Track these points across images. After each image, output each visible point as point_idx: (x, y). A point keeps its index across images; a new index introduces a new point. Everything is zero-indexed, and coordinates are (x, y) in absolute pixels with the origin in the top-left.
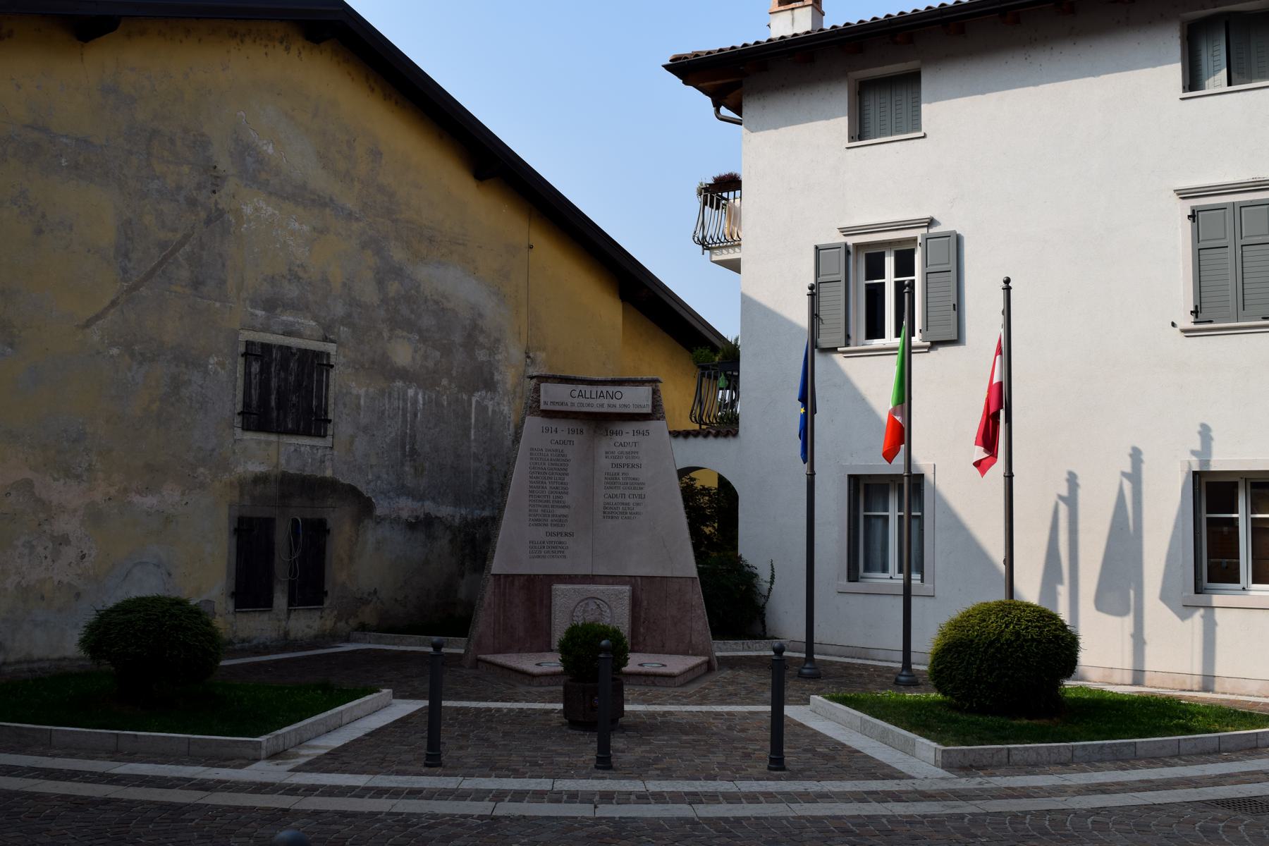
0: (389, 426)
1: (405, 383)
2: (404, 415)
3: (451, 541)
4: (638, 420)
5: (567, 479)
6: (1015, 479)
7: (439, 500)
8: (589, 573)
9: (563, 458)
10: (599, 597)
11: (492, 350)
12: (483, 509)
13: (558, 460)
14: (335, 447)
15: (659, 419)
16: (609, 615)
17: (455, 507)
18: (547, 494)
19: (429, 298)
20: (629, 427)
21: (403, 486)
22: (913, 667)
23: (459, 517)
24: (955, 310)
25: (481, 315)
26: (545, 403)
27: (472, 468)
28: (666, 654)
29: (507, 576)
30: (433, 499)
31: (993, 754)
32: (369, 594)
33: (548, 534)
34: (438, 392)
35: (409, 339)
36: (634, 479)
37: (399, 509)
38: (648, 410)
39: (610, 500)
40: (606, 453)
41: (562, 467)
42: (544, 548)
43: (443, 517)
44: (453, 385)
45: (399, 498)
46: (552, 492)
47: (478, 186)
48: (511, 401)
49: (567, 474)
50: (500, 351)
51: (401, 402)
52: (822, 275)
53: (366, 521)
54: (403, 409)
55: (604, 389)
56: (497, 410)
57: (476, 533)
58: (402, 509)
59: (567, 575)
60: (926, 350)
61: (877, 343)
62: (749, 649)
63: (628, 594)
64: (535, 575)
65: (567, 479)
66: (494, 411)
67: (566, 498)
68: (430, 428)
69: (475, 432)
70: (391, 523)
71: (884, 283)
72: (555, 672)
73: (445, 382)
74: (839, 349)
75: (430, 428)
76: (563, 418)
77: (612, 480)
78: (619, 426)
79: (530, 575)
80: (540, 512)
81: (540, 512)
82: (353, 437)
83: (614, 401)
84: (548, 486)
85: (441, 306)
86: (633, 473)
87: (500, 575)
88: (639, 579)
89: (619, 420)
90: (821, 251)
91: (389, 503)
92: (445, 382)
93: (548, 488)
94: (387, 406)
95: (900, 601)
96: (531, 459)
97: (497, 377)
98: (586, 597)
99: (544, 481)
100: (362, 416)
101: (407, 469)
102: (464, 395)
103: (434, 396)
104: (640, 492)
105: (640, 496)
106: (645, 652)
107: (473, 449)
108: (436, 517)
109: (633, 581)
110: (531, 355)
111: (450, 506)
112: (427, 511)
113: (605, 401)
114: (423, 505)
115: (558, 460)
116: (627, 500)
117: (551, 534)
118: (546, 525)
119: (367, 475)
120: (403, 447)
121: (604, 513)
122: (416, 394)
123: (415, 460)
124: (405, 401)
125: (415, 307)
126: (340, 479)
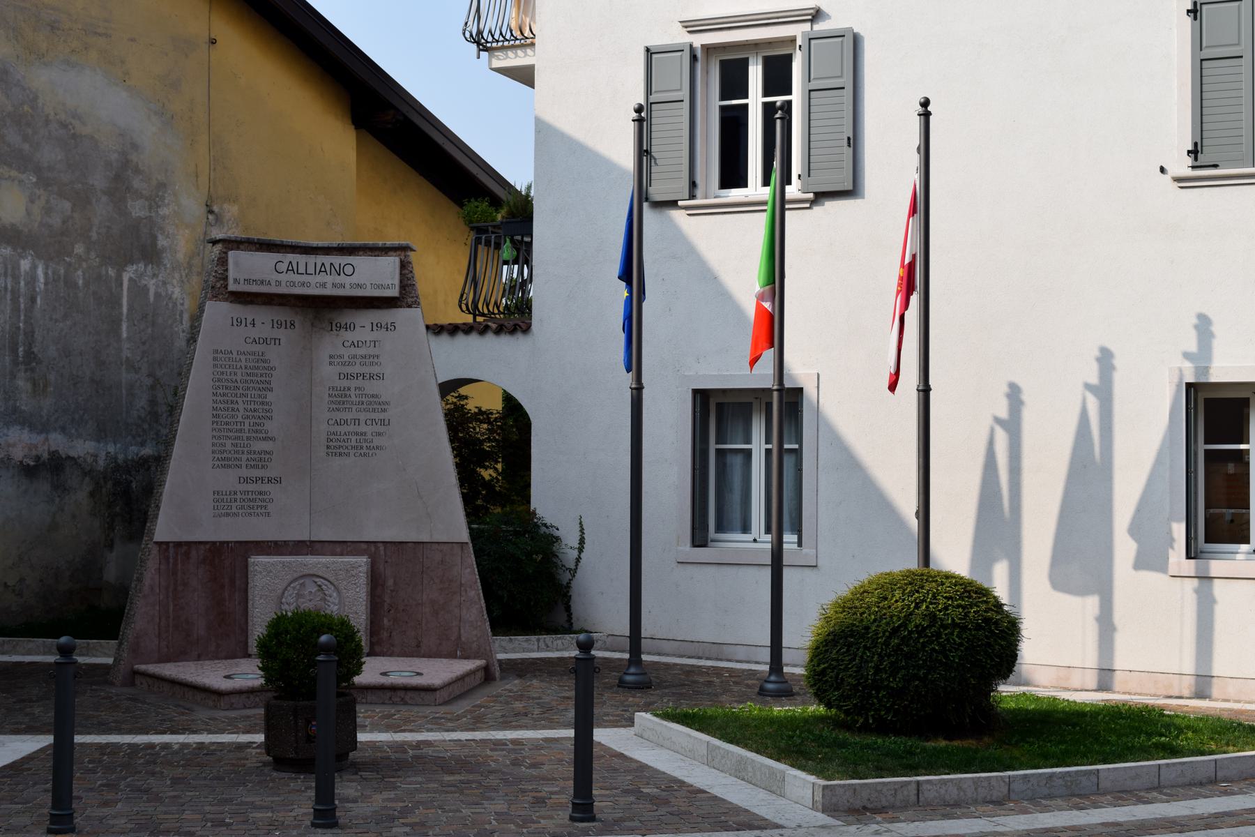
1: (14, 249)
2: (15, 300)
3: (92, 495)
4: (378, 307)
5: (270, 397)
6: (933, 395)
7: (73, 431)
8: (306, 538)
9: (266, 365)
10: (320, 574)
11: (154, 201)
12: (143, 444)
13: (258, 368)
15: (410, 306)
16: (337, 601)
17: (99, 442)
19: (51, 117)
20: (366, 318)
21: (15, 410)
22: (786, 670)
23: (104, 458)
24: (849, 146)
25: (135, 146)
26: (235, 280)
27: (124, 381)
28: (424, 657)
29: (179, 544)
30: (63, 429)
31: (896, 790)
33: (242, 480)
34: (70, 264)
35: (21, 181)
36: (373, 396)
37: (9, 445)
38: (394, 292)
40: (331, 357)
41: (263, 379)
42: (235, 501)
43: (79, 457)
44: (93, 255)
45: (8, 429)
46: (248, 417)
48: (185, 280)
49: (271, 390)
50: (166, 201)
51: (9, 280)
52: (655, 92)
54: (13, 291)
55: (327, 260)
56: (163, 294)
57: (131, 482)
58: (14, 445)
59: (271, 542)
60: (808, 205)
61: (735, 194)
62: (548, 648)
63: (364, 569)
64: (222, 543)
65: (270, 397)
66: (157, 295)
67: (268, 425)
68: (56, 321)
69: (128, 327)
71: (746, 106)
72: (253, 688)
73: (79, 249)
74: (680, 203)
75: (56, 321)
76: (264, 304)
77: (340, 398)
78: (348, 317)
79: (214, 543)
80: (229, 447)
81: (229, 447)
83: (341, 279)
84: (241, 407)
85: (72, 131)
86: (371, 387)
87: (167, 543)
88: (382, 548)
89: (351, 308)
90: (654, 56)
92: (79, 249)
95: (767, 574)
96: (215, 366)
97: (162, 242)
98: (301, 574)
99: (235, 399)
101: (20, 383)
102: (110, 269)
103: (62, 271)
104: (382, 416)
105: (383, 422)
106: (391, 655)
107: (126, 353)
108: (69, 457)
109: (373, 549)
110: (215, 208)
111: (91, 441)
112: (53, 449)
113: (328, 279)
114: (47, 439)
115: (258, 368)
116: (363, 428)
117: (246, 480)
118: (239, 467)
120: (14, 351)
121: (328, 447)
122: (34, 267)
123: (33, 370)
124: (16, 278)
125: (30, 131)
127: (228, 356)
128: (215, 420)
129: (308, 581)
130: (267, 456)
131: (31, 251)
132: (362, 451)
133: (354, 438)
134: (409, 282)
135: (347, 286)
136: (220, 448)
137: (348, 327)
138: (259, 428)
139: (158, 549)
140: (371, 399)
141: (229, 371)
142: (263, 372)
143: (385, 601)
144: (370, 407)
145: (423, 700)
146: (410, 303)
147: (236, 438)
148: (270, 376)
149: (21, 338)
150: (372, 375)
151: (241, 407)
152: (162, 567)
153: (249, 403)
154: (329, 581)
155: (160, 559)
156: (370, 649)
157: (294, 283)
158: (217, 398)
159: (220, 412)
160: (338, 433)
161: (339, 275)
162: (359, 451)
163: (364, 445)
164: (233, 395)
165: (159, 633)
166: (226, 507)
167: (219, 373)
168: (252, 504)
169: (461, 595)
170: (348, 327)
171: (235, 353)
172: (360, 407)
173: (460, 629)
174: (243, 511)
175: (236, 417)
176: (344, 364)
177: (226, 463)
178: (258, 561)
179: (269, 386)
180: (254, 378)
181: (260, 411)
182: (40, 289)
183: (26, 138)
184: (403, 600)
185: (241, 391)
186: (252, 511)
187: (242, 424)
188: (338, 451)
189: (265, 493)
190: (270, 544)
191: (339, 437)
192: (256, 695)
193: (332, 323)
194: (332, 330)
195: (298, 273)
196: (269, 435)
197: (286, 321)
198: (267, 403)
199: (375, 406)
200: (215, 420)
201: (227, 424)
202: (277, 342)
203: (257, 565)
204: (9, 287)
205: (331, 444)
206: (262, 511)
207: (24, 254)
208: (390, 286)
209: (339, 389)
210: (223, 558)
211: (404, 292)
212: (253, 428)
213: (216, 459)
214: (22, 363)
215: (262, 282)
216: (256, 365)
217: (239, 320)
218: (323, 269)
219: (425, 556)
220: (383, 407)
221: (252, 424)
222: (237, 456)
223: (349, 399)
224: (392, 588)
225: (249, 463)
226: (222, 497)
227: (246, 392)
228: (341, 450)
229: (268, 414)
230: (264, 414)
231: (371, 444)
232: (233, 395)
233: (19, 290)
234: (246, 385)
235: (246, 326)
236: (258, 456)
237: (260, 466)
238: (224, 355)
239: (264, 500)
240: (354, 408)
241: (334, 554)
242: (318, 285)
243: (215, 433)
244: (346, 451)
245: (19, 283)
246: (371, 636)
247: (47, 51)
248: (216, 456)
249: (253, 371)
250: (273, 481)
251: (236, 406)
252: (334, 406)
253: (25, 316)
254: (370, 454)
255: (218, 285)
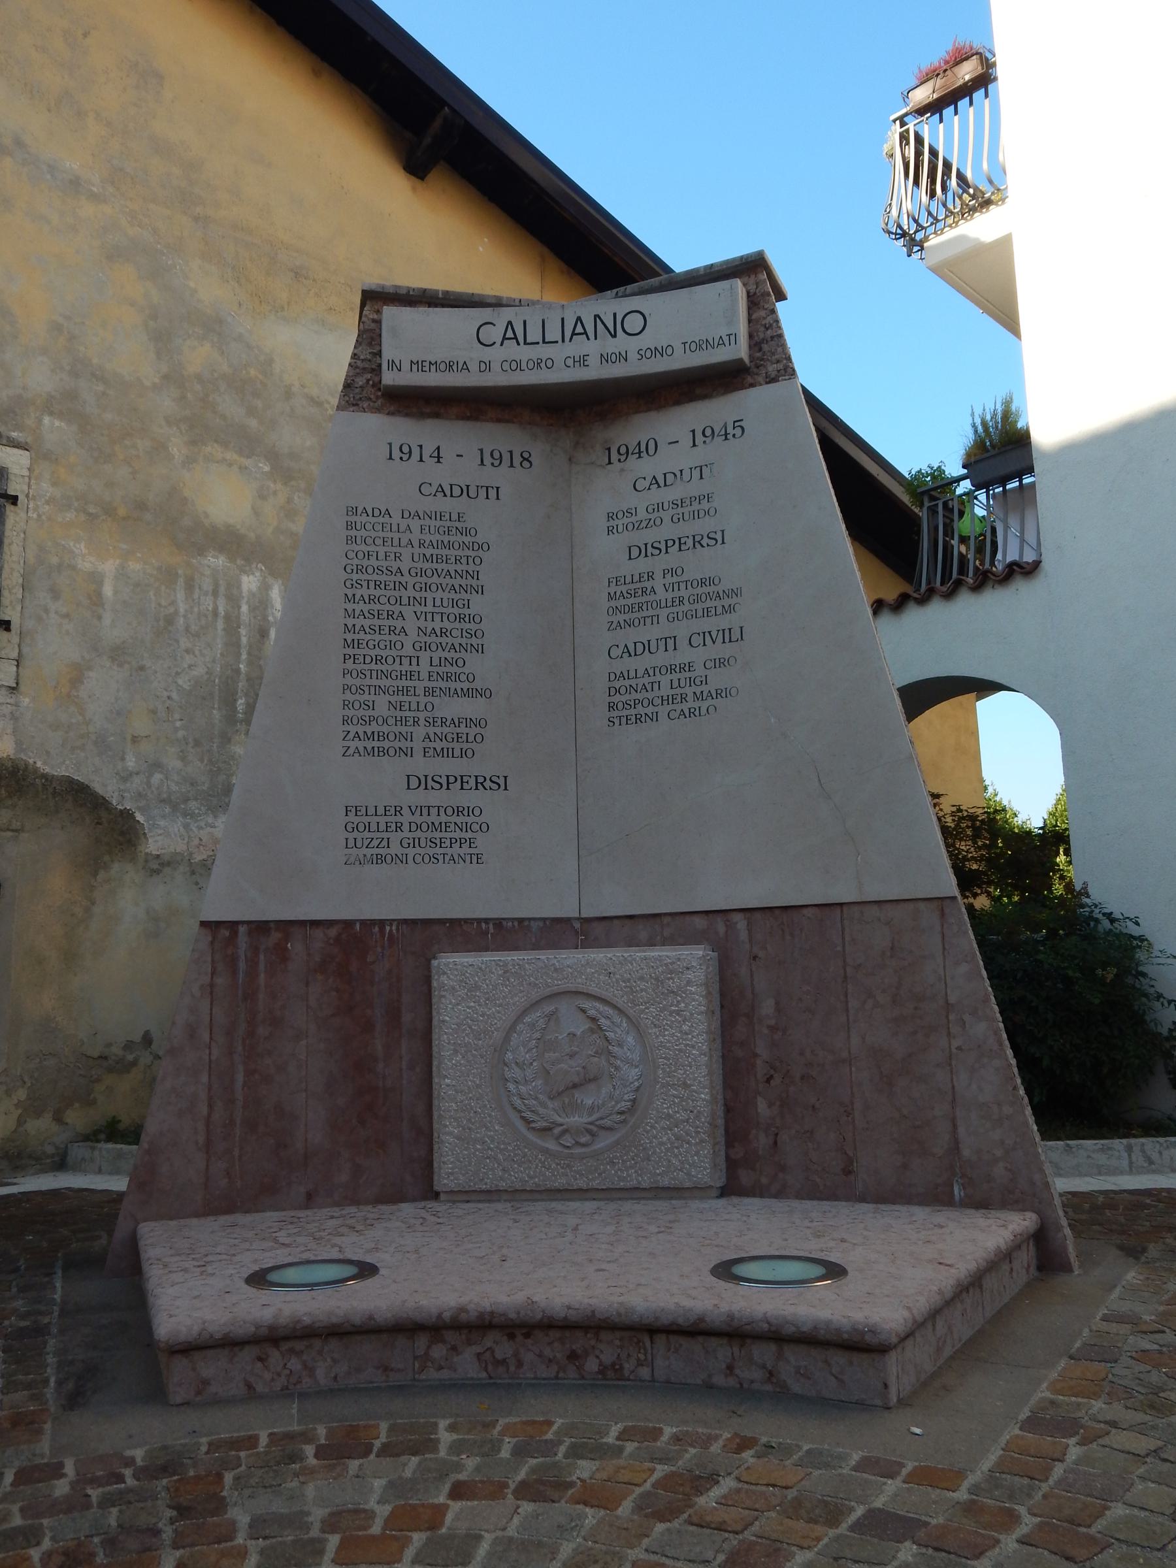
0: (187, 651)
5: (478, 604)
9: (467, 539)
10: (593, 989)
13: (450, 545)
14: (22, 688)
15: (772, 380)
16: (636, 1056)
18: (411, 652)
28: (863, 1199)
29: (260, 928)
32: (129, 1046)
33: (414, 783)
36: (702, 583)
39: (630, 664)
40: (610, 517)
41: (459, 568)
42: (399, 827)
45: (215, 817)
46: (427, 647)
47: (414, 189)
49: (480, 590)
53: (116, 867)
54: (227, 618)
59: (487, 921)
62: (1151, 1166)
63: (698, 975)
64: (367, 924)
65: (478, 604)
67: (474, 664)
70: (193, 873)
72: (272, 1328)
79: (348, 924)
82: (77, 675)
83: (621, 343)
84: (411, 625)
86: (697, 564)
87: (233, 925)
88: (741, 922)
91: (186, 826)
93: (413, 633)
94: (182, 607)
98: (548, 991)
99: (397, 609)
100: (107, 619)
104: (724, 622)
105: (727, 636)
106: (779, 1195)
109: (721, 928)
113: (591, 348)
115: (450, 545)
116: (685, 655)
117: (424, 782)
119: (123, 759)
121: (611, 707)
122: (265, 588)
124: (234, 600)
125: (259, 403)
126: (39, 764)
127: (381, 519)
128: (350, 651)
129: (565, 1007)
130: (473, 731)
131: (260, 565)
132: (685, 707)
133: (665, 680)
134: (769, 332)
135: (633, 356)
136: (361, 713)
137: (643, 448)
138: (454, 669)
139: (210, 939)
140: (699, 590)
141: (382, 551)
142: (460, 553)
143: (756, 1055)
144: (699, 606)
145: (841, 1382)
146: (773, 375)
147: (405, 691)
148: (477, 561)
149: (242, 684)
150: (698, 538)
151: (411, 625)
152: (219, 981)
153: (429, 616)
154: (615, 1007)
155: (213, 961)
156: (728, 1179)
157: (519, 364)
158: (355, 606)
159: (362, 635)
160: (632, 674)
161: (614, 336)
162: (678, 707)
163: (689, 691)
164: (393, 601)
165: (209, 1143)
166: (375, 843)
167: (360, 555)
168: (438, 835)
169: (949, 1034)
170: (643, 448)
171: (396, 516)
172: (675, 609)
173: (955, 1126)
174: (418, 850)
175: (399, 646)
176: (637, 527)
177: (376, 744)
178: (447, 965)
179: (474, 583)
180: (439, 567)
181: (455, 633)
182: (274, 617)
183: (251, 412)
184: (802, 1054)
185: (411, 592)
186: (438, 850)
187: (414, 661)
188: (633, 712)
189: (470, 811)
190: (484, 925)
191: (633, 682)
192: (292, 1351)
193: (609, 449)
194: (610, 463)
195: (525, 343)
196: (478, 684)
197: (511, 452)
198: (472, 619)
199: (709, 604)
200: (350, 651)
201: (377, 660)
202: (492, 493)
203: (444, 973)
204: (221, 610)
205: (617, 698)
206: (462, 852)
207: (247, 568)
208: (726, 339)
209: (628, 579)
210: (370, 959)
211: (758, 355)
212: (441, 670)
213: (351, 736)
214: (241, 722)
215: (450, 366)
216: (446, 539)
217: (406, 449)
218: (579, 329)
219: (847, 939)
220: (726, 602)
221: (436, 662)
222: (404, 729)
223: (652, 597)
224: (772, 1022)
225: (432, 745)
226: (366, 820)
227: (423, 594)
228: (640, 709)
229: (474, 641)
230: (464, 641)
231: (704, 688)
232: (393, 601)
233: (238, 617)
234: (424, 579)
235: (421, 460)
236: (452, 729)
237: (457, 753)
238: (370, 519)
239: (468, 827)
240: (663, 613)
241: (632, 942)
242: (570, 362)
243: (349, 680)
244: (650, 710)
245: (239, 607)
246: (729, 1144)
247: (289, 303)
248: (353, 729)
249: (435, 552)
250: (488, 784)
251: (399, 624)
252: (621, 617)
253: (249, 654)
254: (704, 711)
255: (360, 381)
